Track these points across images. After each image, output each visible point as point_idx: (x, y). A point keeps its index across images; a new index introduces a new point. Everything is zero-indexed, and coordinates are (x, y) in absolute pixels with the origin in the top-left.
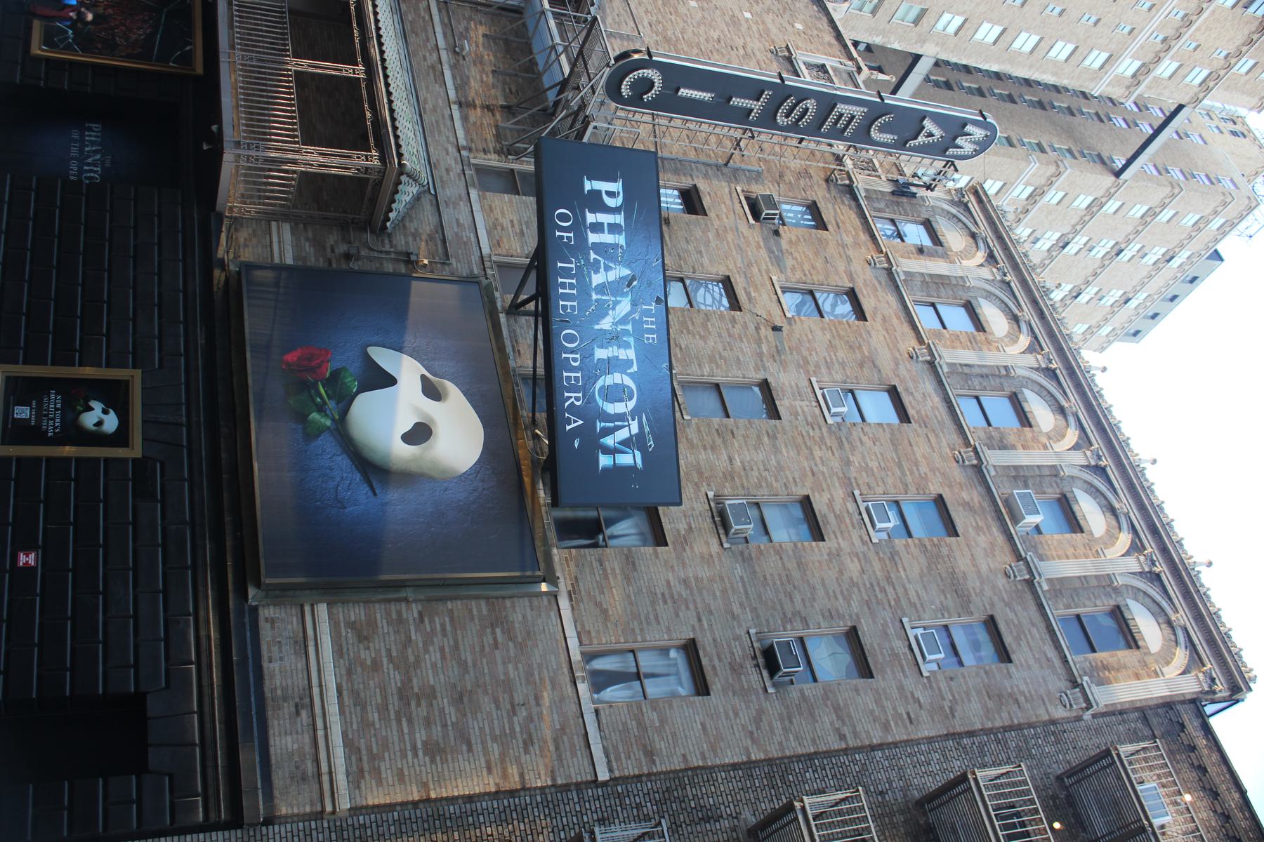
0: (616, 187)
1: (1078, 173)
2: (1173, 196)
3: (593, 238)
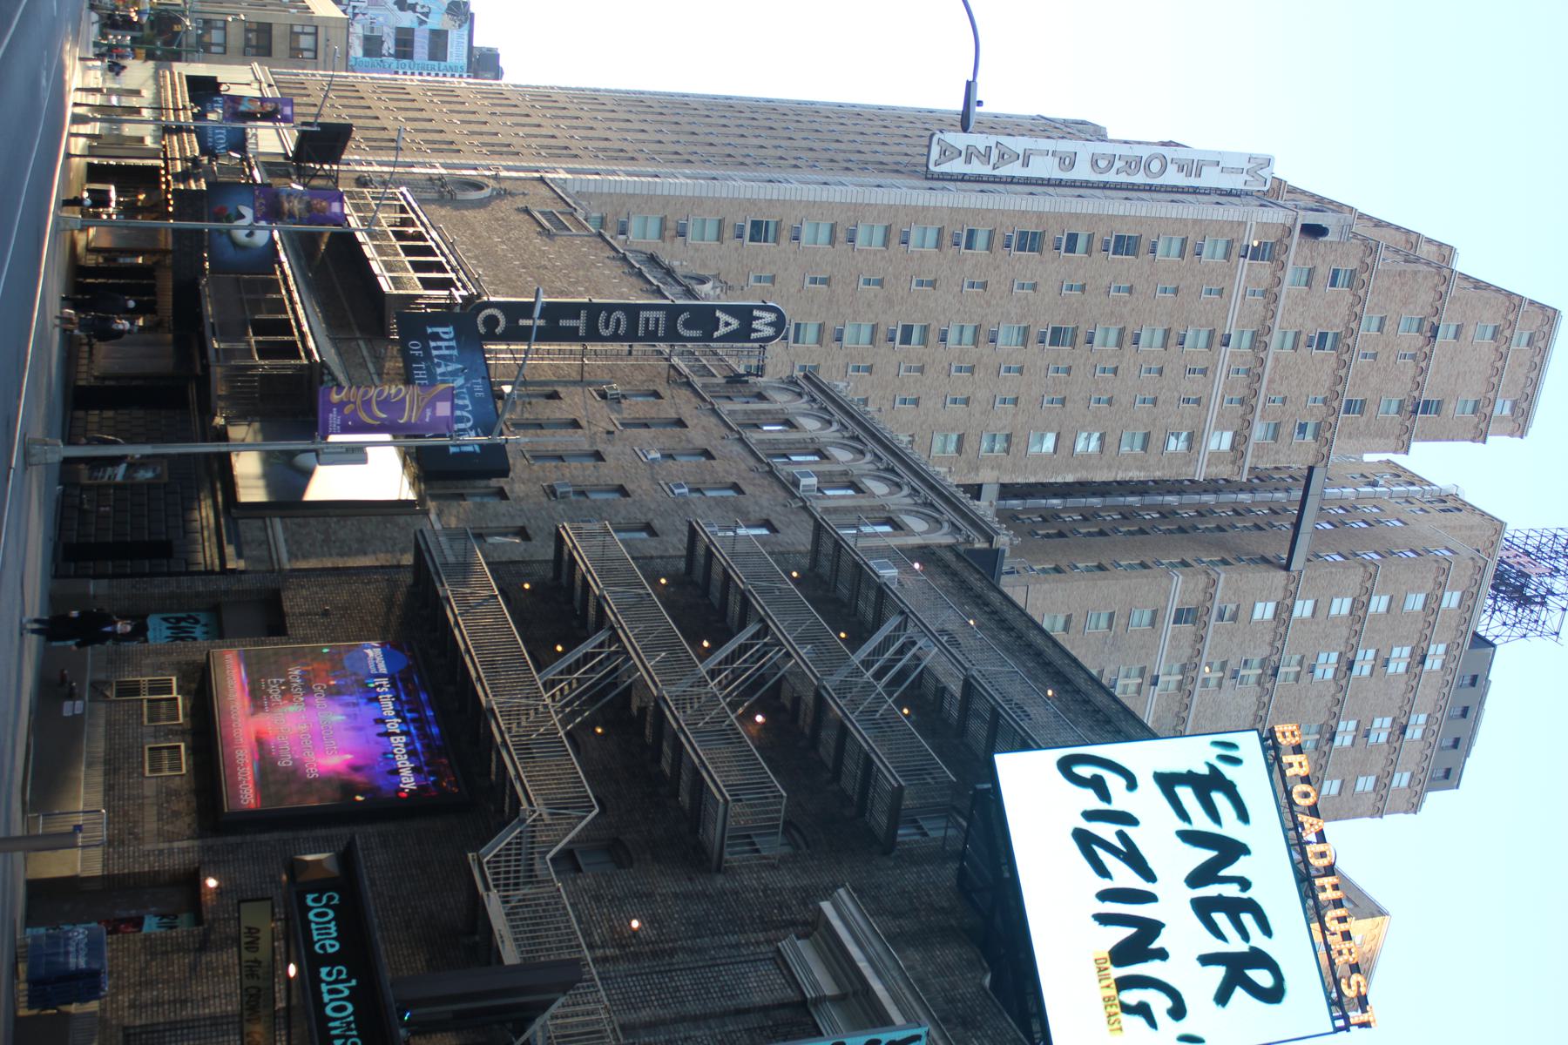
0: (450, 329)
1: (1235, 576)
2: (1372, 577)
3: (435, 353)
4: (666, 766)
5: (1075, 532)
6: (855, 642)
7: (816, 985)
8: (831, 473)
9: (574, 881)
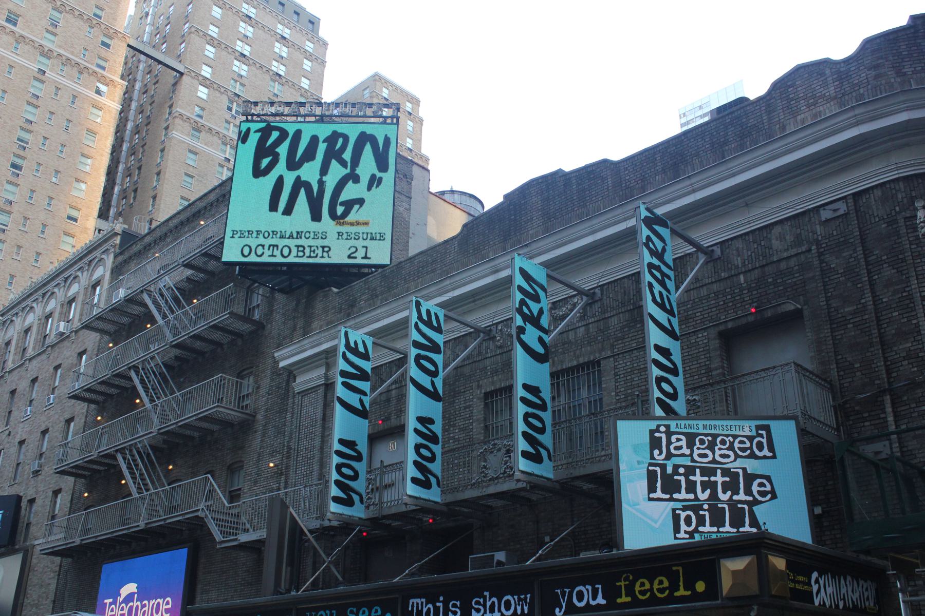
1: (180, 102)
2: (197, 31)
4: (196, 434)
5: (136, 183)
6: (153, 321)
7: (319, 378)
8: (61, 314)
9: (244, 493)
